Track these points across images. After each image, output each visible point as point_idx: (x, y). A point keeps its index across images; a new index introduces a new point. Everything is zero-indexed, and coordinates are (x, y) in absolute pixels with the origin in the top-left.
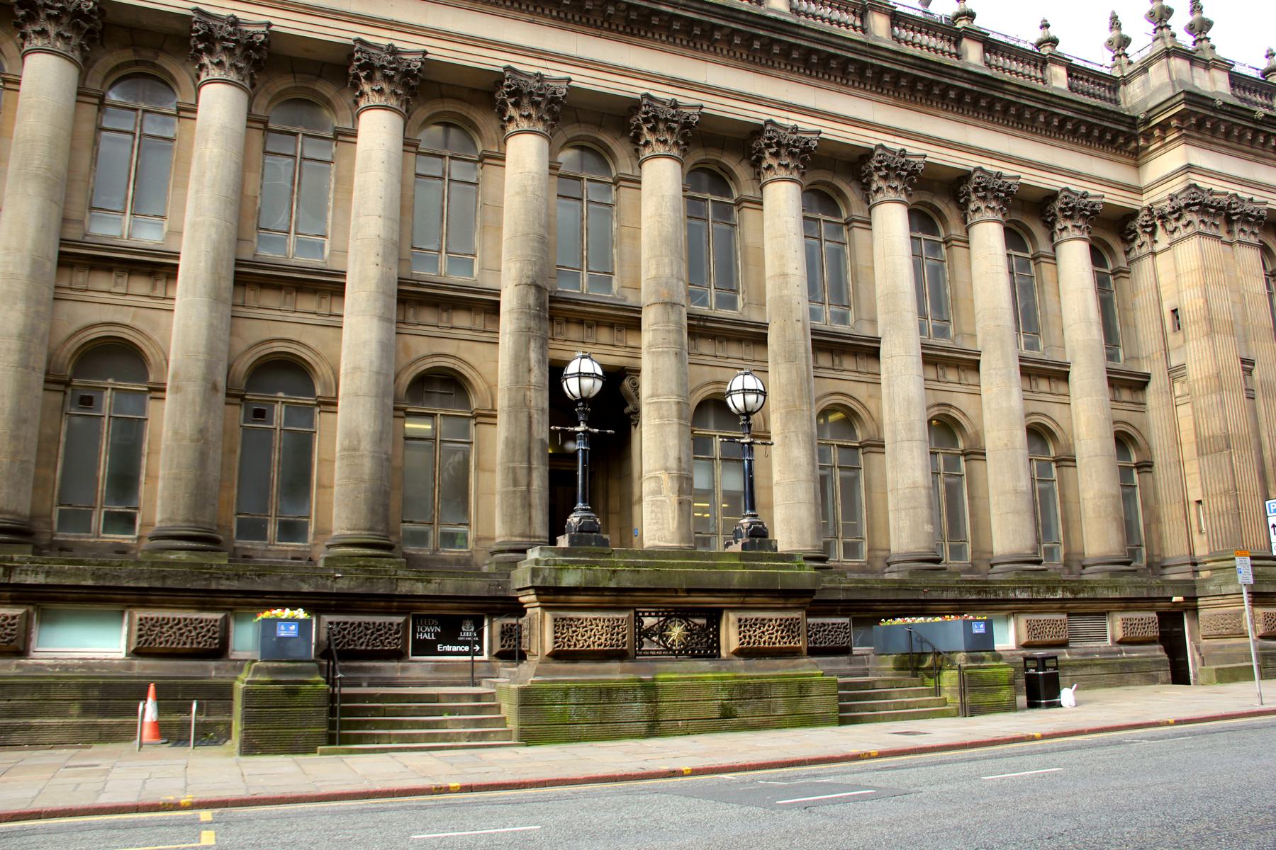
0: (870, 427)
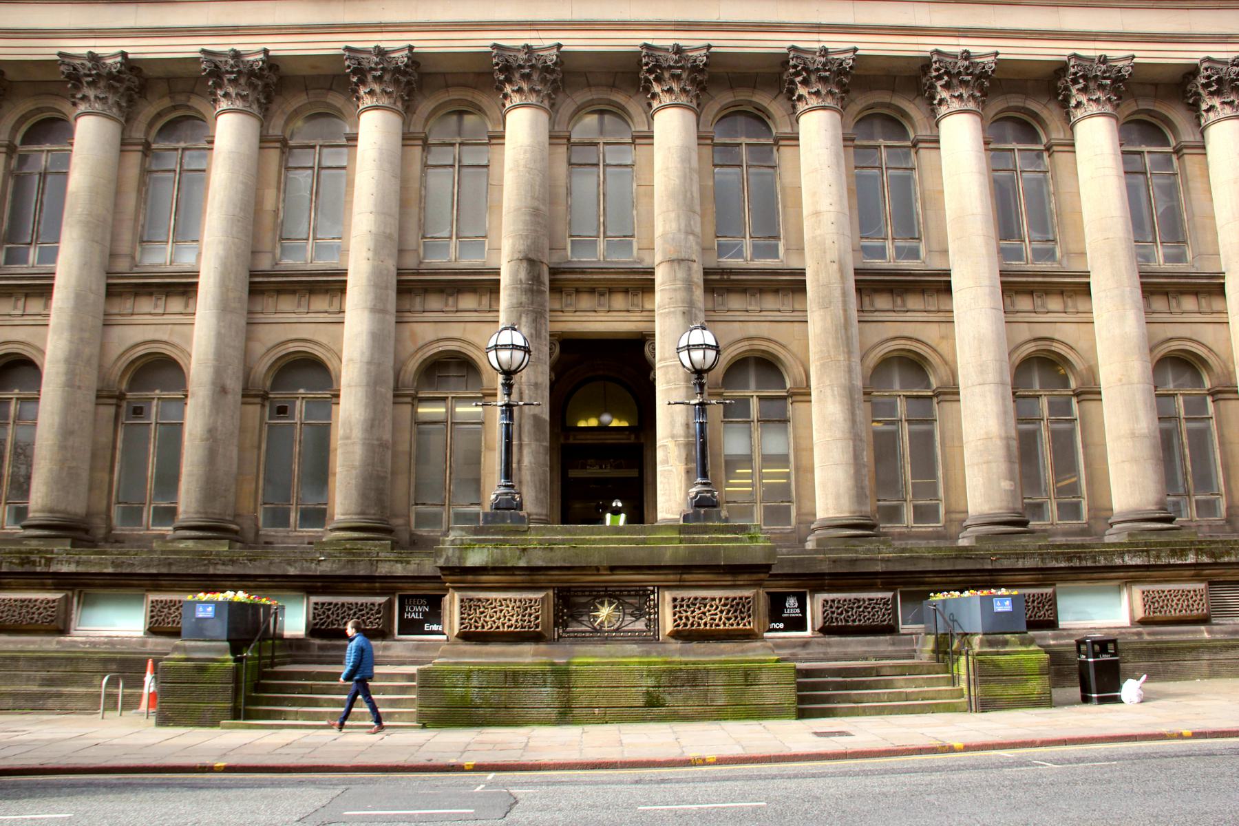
0: (943, 371)
